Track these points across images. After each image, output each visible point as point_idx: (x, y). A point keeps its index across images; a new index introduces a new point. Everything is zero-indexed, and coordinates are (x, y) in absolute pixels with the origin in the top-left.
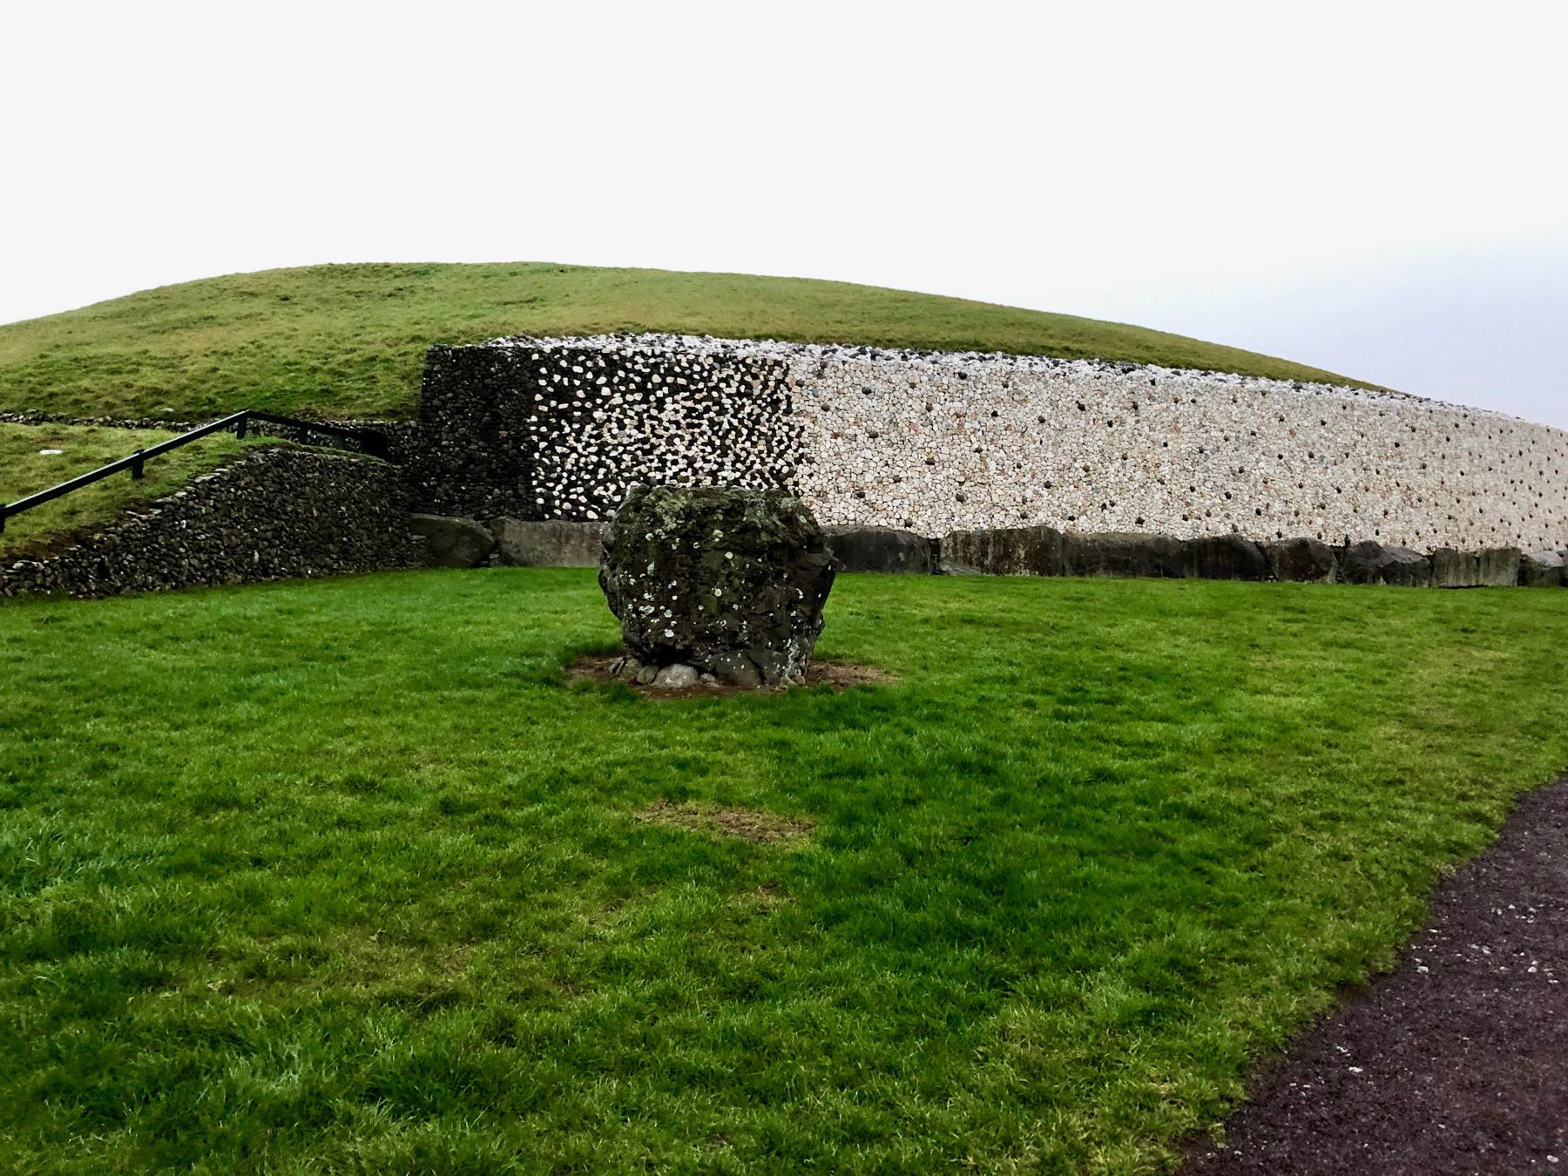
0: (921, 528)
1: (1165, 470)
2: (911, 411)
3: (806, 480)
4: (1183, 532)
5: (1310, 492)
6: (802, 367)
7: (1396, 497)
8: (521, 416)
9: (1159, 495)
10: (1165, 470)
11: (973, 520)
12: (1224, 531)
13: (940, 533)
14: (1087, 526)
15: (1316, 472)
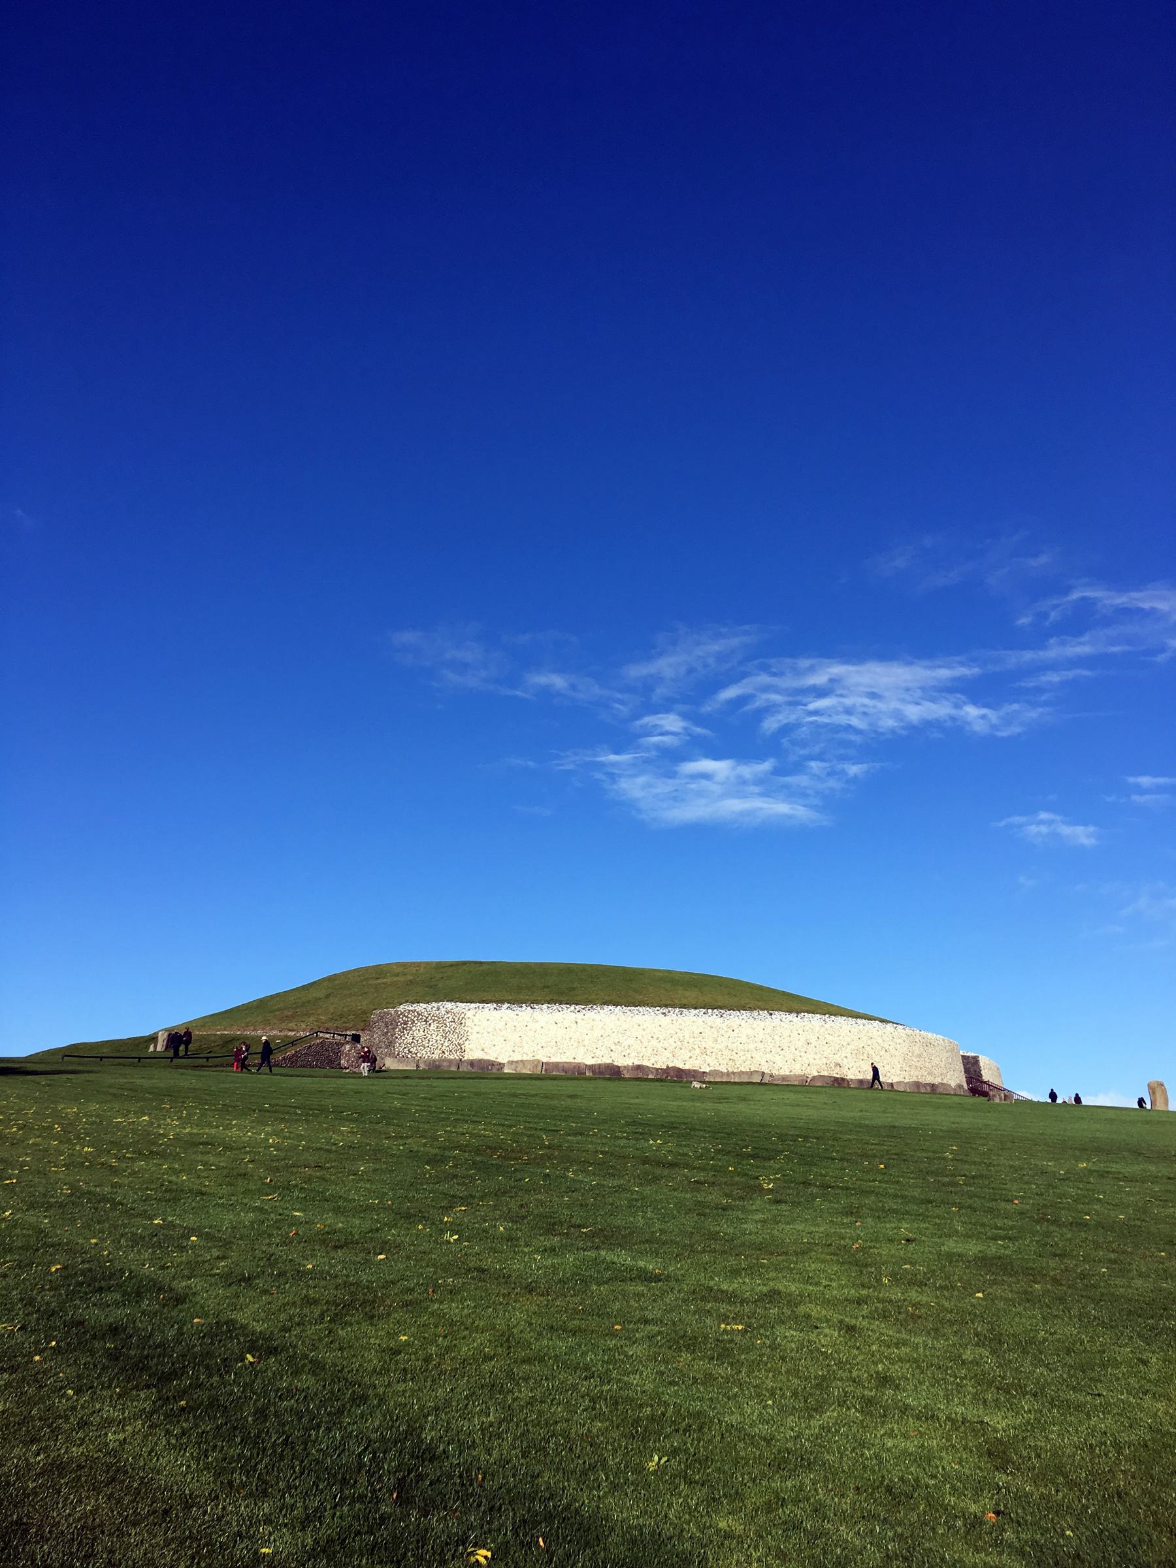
0: (500, 1060)
1: (586, 1043)
2: (501, 1025)
3: (467, 1046)
4: (590, 1062)
5: (650, 1051)
6: (469, 1014)
7: (698, 1051)
8: (394, 1029)
9: (582, 1050)
10: (586, 1043)
11: (517, 1057)
12: (609, 1061)
13: (505, 1061)
14: (554, 1060)
15: (654, 1042)
